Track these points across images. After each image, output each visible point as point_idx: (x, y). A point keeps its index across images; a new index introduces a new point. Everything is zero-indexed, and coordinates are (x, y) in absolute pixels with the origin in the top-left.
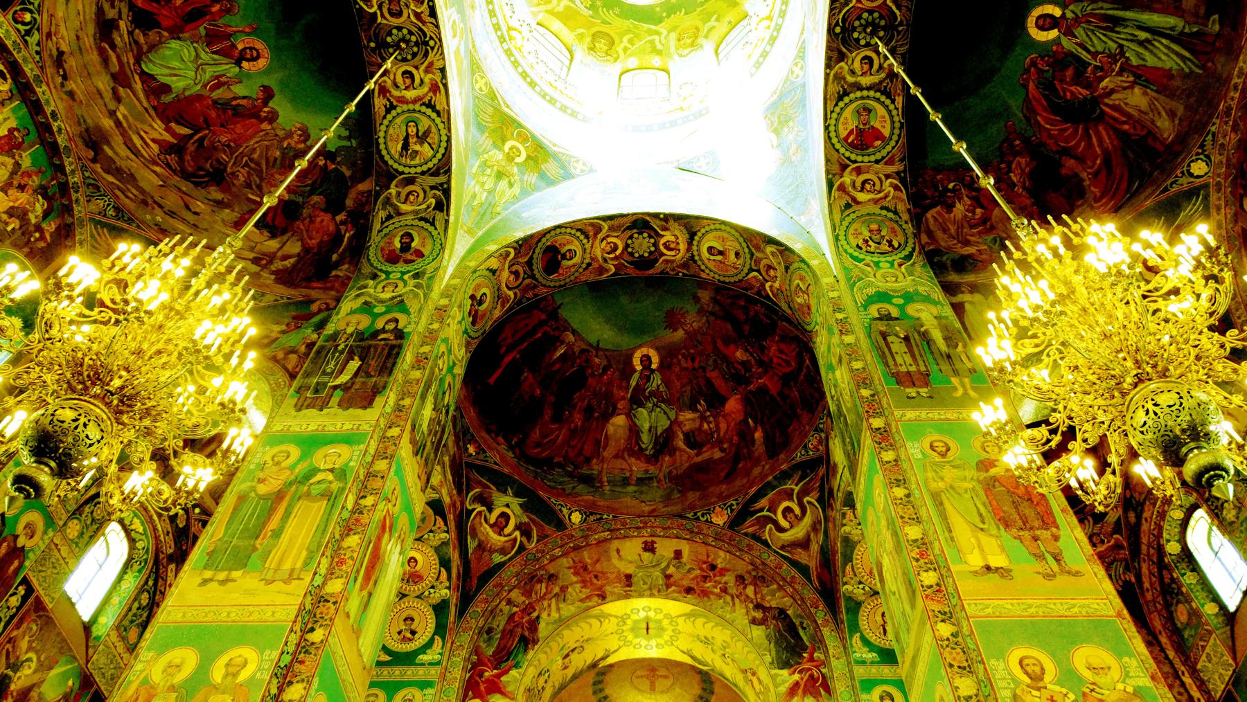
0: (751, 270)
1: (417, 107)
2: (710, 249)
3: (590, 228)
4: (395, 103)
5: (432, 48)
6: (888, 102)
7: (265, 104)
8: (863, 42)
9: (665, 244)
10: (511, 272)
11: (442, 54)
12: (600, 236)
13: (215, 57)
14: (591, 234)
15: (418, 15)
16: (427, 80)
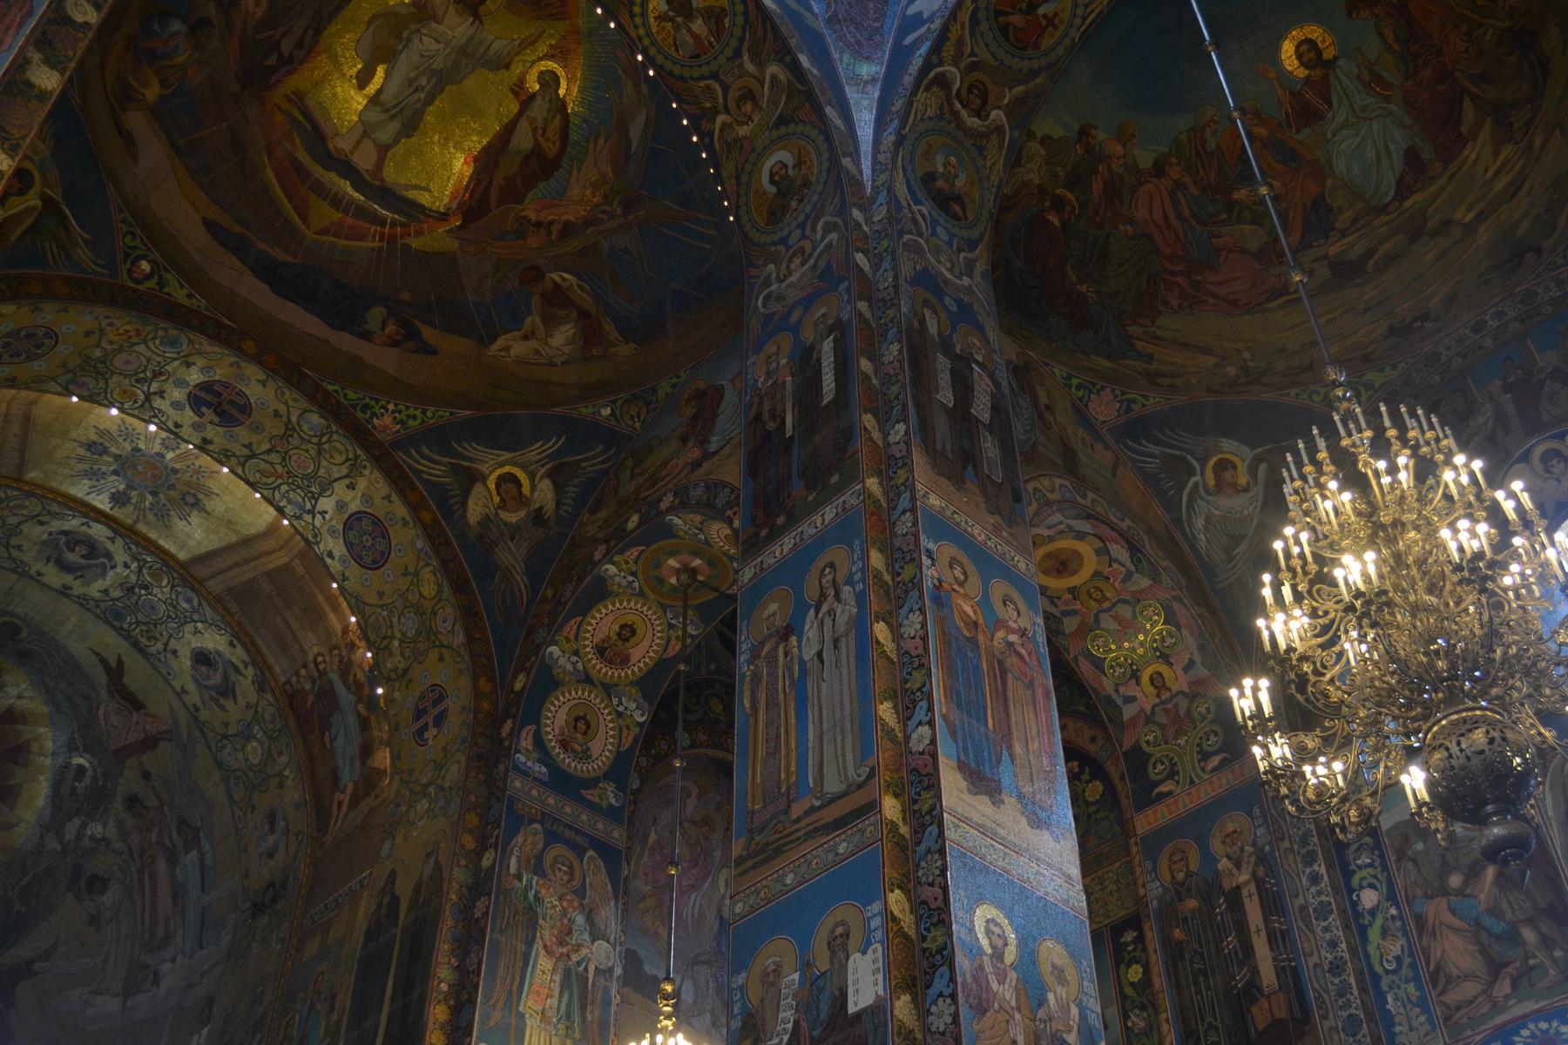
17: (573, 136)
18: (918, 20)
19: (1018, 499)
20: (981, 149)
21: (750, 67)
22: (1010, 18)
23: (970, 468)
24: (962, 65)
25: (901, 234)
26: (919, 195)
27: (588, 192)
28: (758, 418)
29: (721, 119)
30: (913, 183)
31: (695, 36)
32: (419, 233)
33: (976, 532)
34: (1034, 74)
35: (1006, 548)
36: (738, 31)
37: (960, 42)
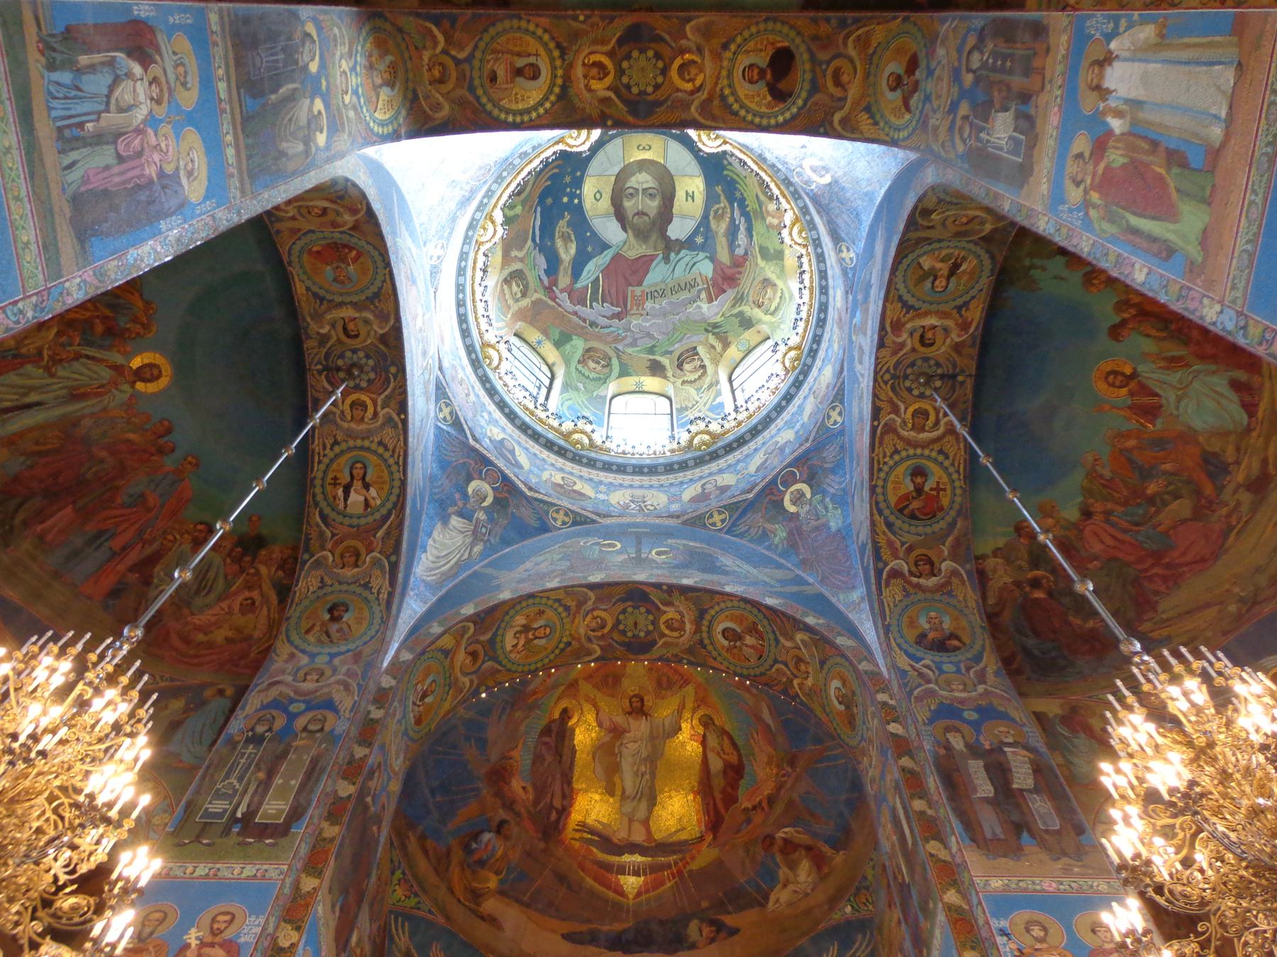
0: (469, 59)
1: (925, 307)
2: (535, 77)
3: (717, 112)
4: (955, 312)
5: (888, 371)
6: (315, 289)
7: (1123, 323)
8: (361, 354)
9: (606, 75)
10: (845, 90)
11: (876, 365)
12: (704, 95)
13: (1158, 391)
14: (716, 102)
15: (896, 410)
16: (905, 336)
17: (740, 743)
18: (864, 546)
19: (1080, 830)
20: (950, 593)
21: (788, 644)
22: (911, 507)
23: (1025, 835)
24: (901, 555)
25: (910, 693)
26: (919, 654)
27: (768, 770)
28: (895, 878)
29: (796, 682)
30: (911, 650)
31: (752, 647)
32: (693, 858)
33: (1045, 886)
34: (952, 525)
35: (1081, 882)
36: (770, 630)
37: (890, 544)
